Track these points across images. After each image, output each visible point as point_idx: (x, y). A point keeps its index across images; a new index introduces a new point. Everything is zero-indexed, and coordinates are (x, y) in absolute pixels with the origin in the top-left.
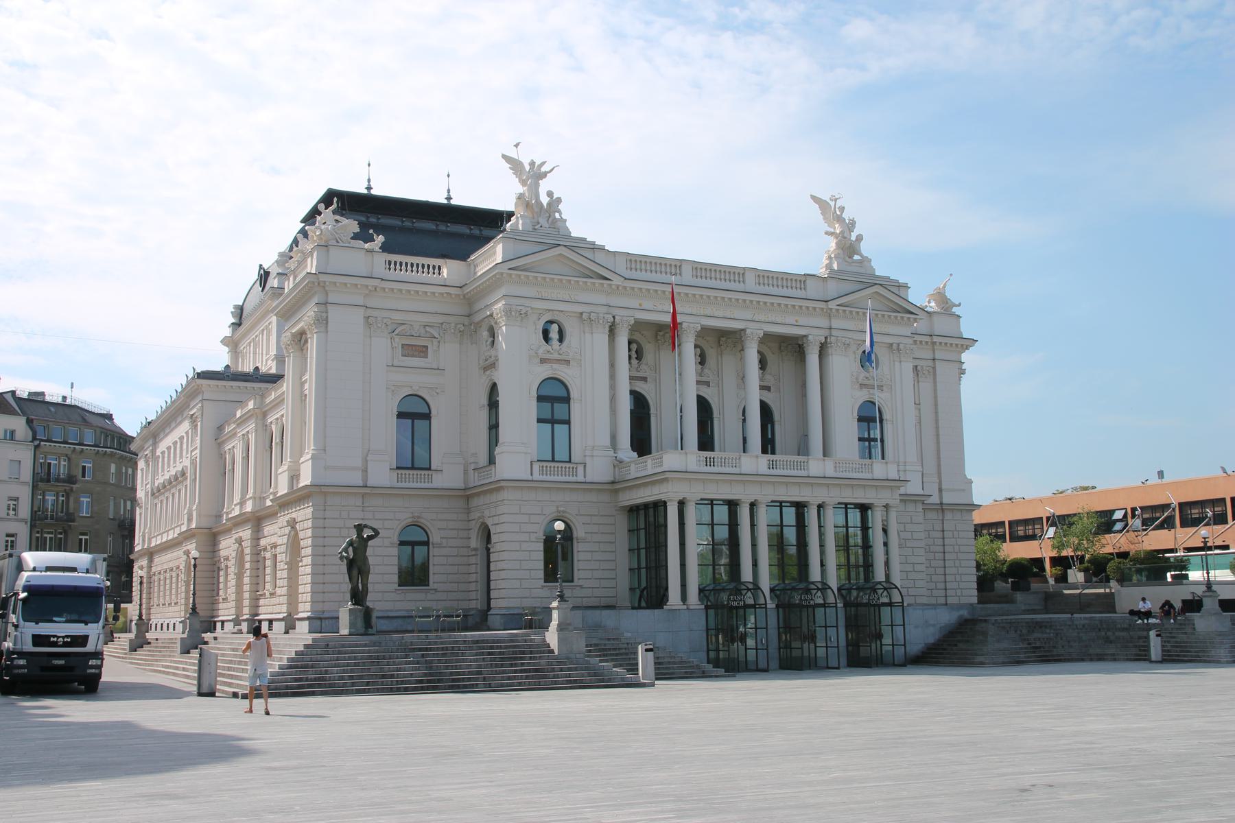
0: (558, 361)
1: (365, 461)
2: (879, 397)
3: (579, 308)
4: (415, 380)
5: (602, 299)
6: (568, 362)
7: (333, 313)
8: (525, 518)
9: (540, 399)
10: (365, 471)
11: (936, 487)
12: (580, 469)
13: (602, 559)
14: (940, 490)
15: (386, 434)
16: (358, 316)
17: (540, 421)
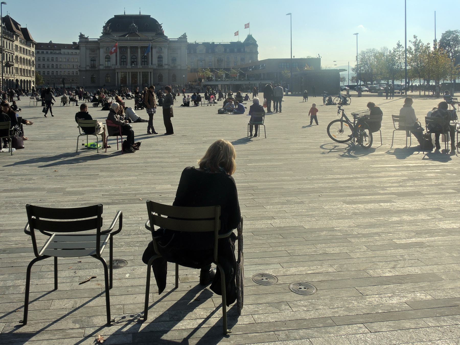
2: (162, 55)
5: (114, 44)
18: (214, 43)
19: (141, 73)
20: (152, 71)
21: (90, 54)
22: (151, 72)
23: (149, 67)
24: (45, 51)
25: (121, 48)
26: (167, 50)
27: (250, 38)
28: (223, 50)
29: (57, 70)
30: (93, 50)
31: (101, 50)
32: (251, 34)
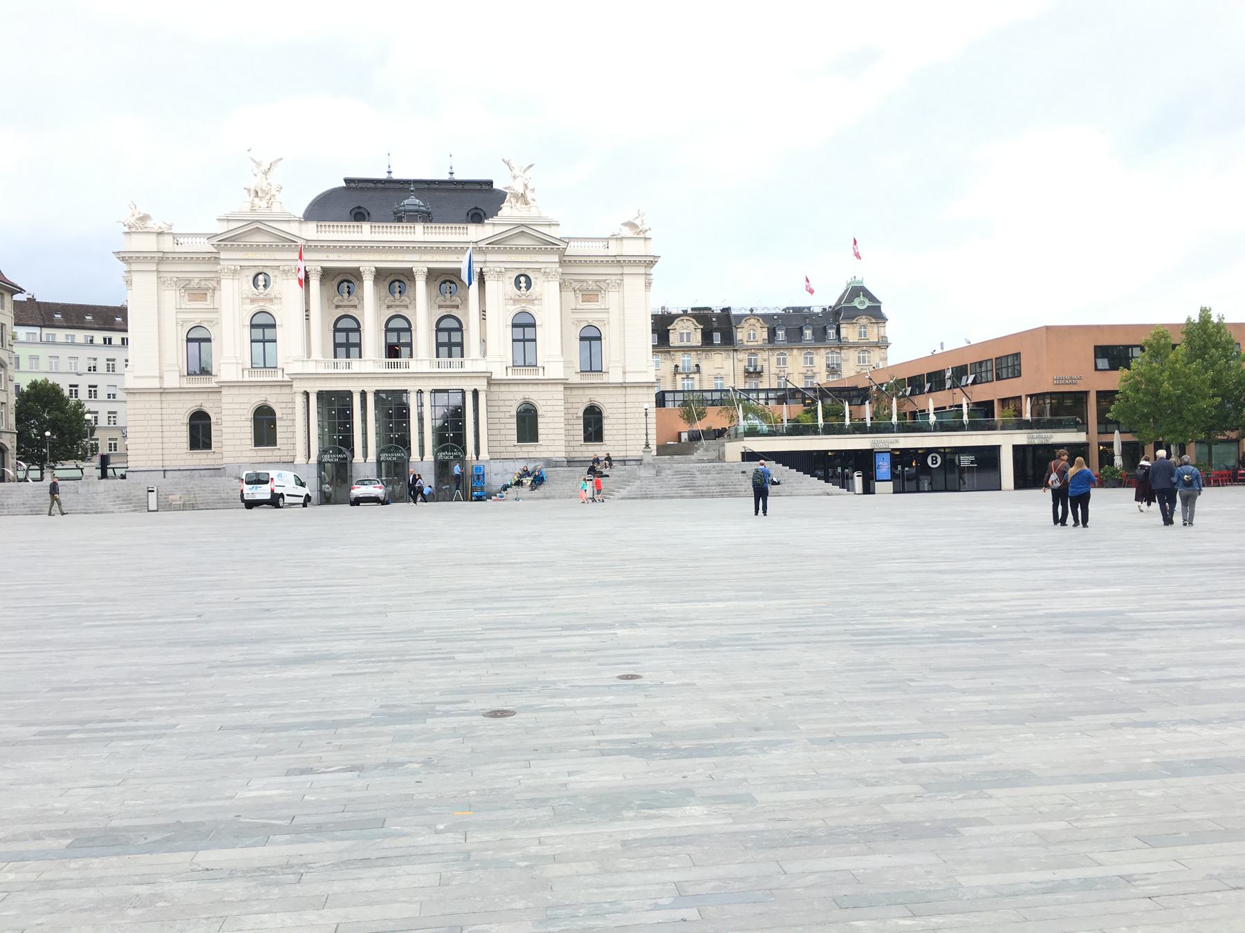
0: (263, 300)
1: (160, 370)
2: (531, 309)
3: (277, 263)
4: (197, 318)
6: (271, 300)
7: (136, 278)
8: (237, 406)
9: (253, 326)
10: (161, 378)
11: (621, 370)
12: (280, 372)
13: (300, 433)
14: (624, 373)
15: (177, 354)
16: (154, 276)
17: (252, 341)
18: (728, 309)
19: (427, 398)
20: (481, 385)
21: (179, 310)
22: (475, 393)
23: (469, 367)
24: (99, 336)
25: (327, 274)
26: (555, 285)
27: (857, 291)
28: (765, 335)
29: (112, 407)
30: (199, 293)
31: (227, 284)
32: (859, 278)
